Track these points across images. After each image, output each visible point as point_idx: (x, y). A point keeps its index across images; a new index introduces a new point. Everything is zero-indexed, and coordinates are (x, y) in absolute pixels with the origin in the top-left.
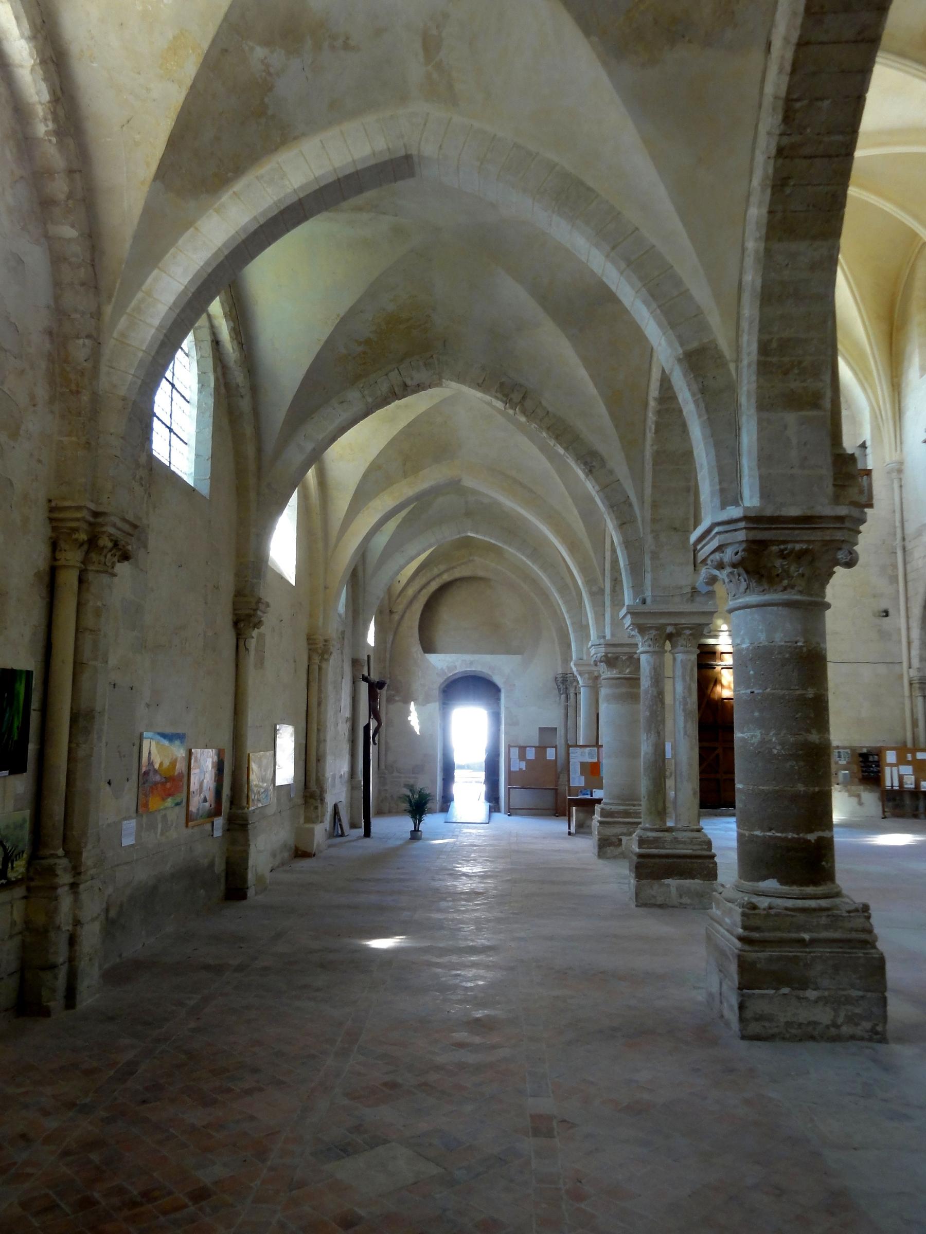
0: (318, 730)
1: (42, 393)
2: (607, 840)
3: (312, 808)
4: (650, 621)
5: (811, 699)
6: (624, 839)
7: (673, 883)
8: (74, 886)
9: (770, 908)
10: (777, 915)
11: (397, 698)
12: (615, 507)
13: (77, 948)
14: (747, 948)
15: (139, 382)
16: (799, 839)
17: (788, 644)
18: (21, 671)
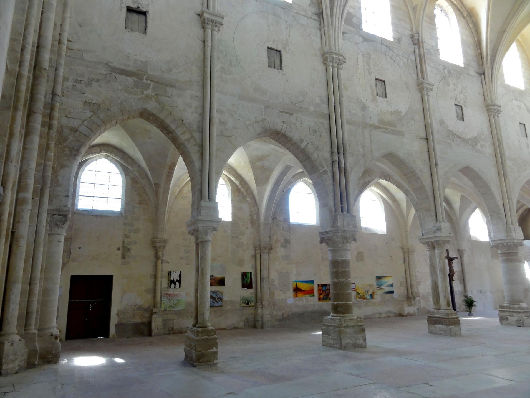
2: (502, 318)
6: (509, 317)
7: (437, 326)
18: (248, 272)
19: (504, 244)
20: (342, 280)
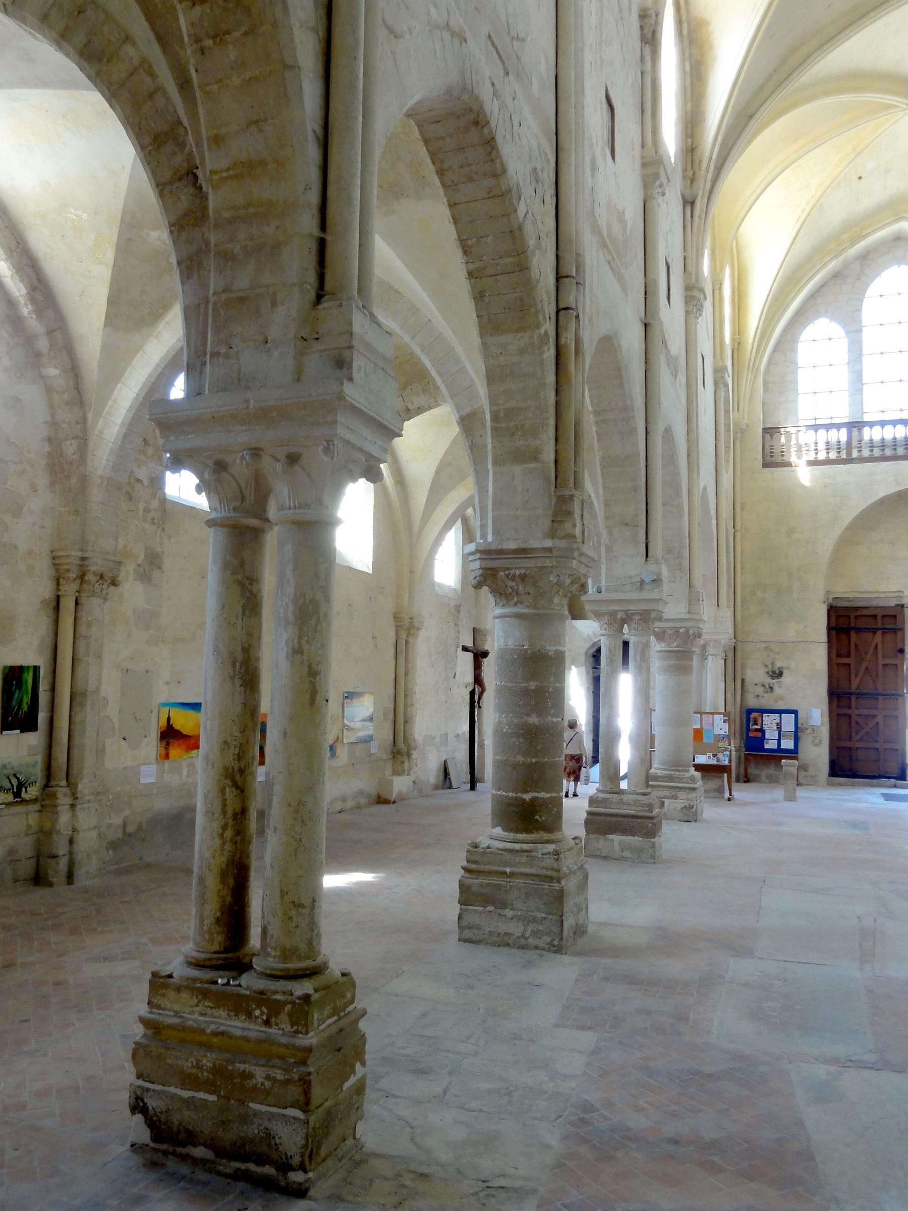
0: (406, 696)
1: (42, 481)
3: (398, 762)
4: (604, 608)
5: (533, 691)
6: (667, 802)
7: (616, 838)
8: (73, 806)
9: (488, 847)
10: (491, 853)
13: (75, 846)
14: (467, 875)
15: (111, 464)
17: (517, 647)
18: (28, 667)
20: (555, 720)
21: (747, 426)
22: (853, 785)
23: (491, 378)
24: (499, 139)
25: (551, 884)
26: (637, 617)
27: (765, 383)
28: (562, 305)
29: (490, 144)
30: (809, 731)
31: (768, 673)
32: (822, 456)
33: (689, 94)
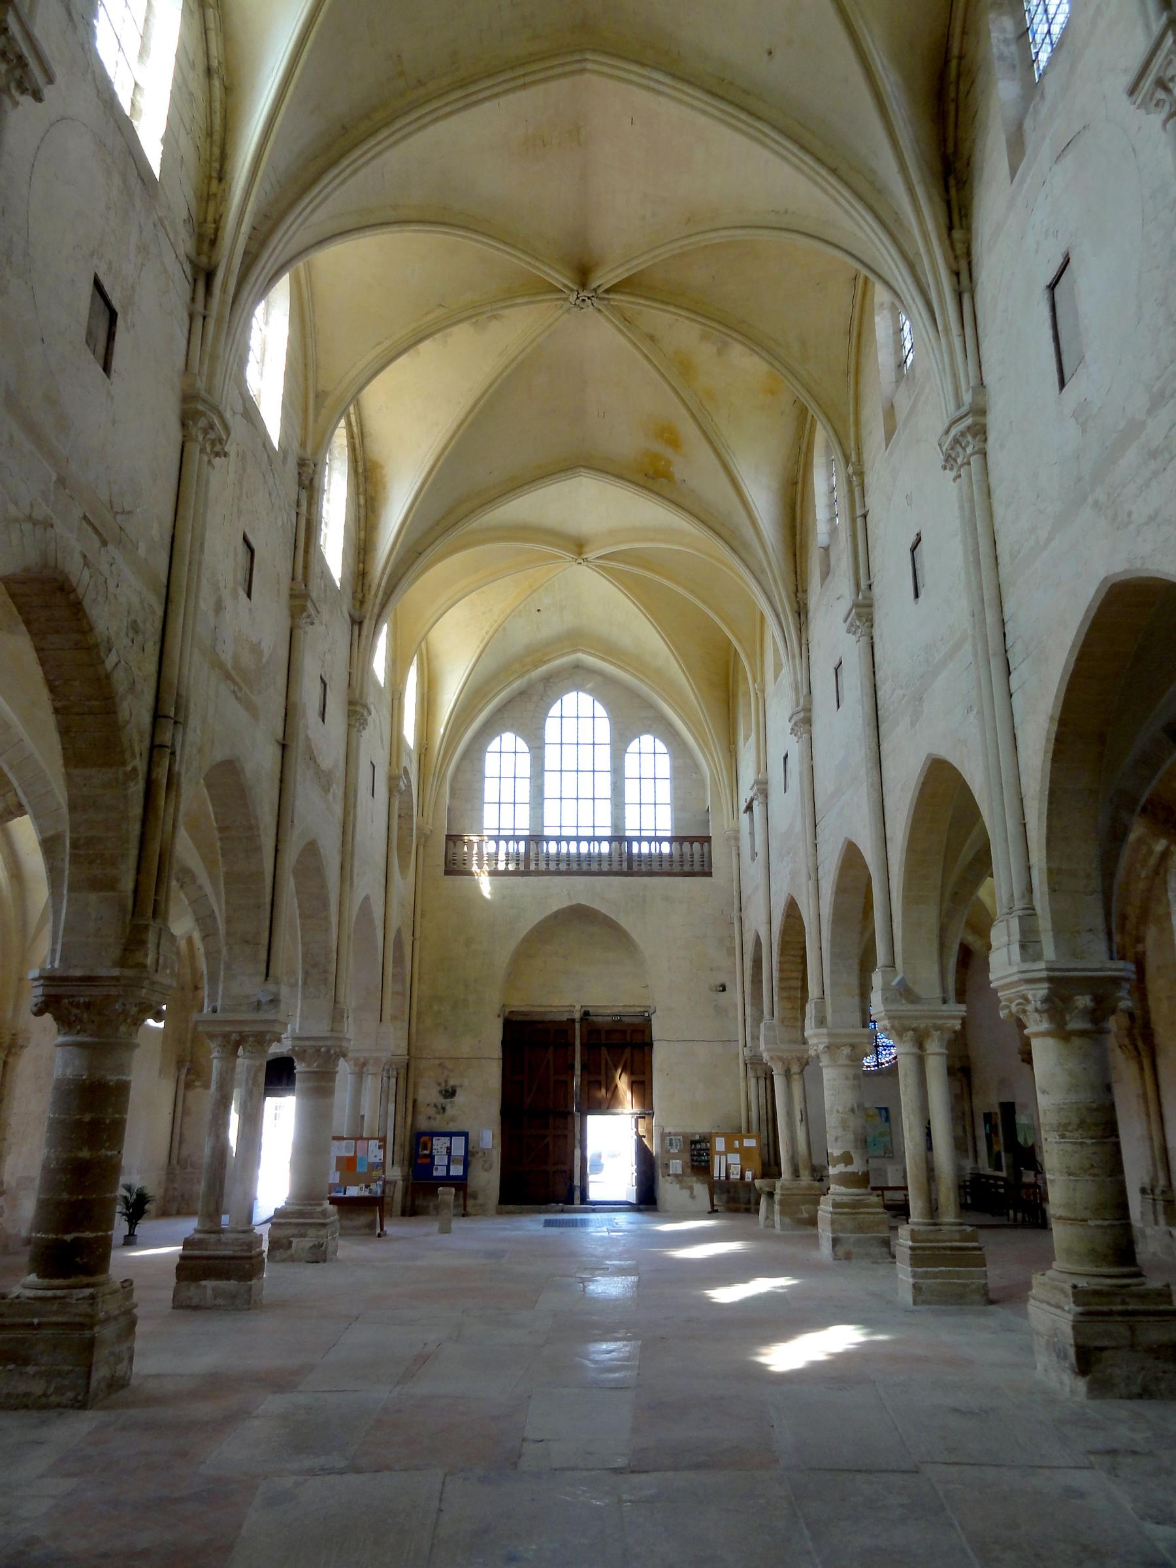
4: (218, 1029)
6: (295, 1241)
7: (209, 1284)
9: (18, 1297)
10: (20, 1303)
11: (197, 1084)
12: (200, 921)
16: (57, 1239)
19: (319, 1050)
20: (109, 1153)
21: (431, 831)
22: (521, 1213)
23: (73, 807)
24: (87, 603)
25: (82, 1332)
26: (251, 1039)
27: (452, 789)
28: (157, 742)
29: (77, 608)
30: (480, 1154)
31: (441, 1092)
32: (501, 866)
33: (362, 524)
